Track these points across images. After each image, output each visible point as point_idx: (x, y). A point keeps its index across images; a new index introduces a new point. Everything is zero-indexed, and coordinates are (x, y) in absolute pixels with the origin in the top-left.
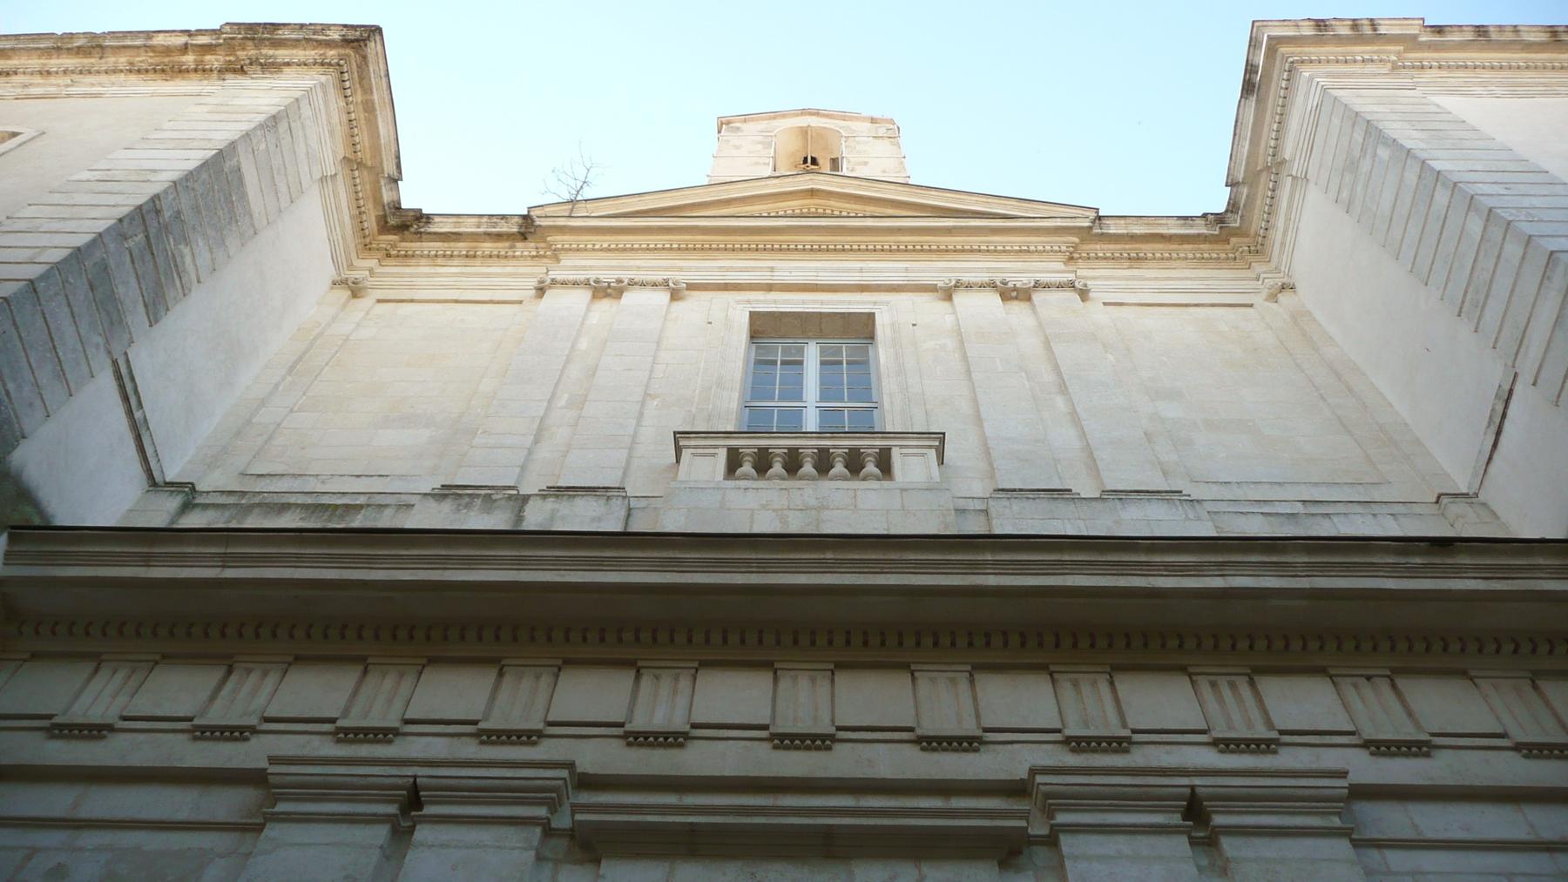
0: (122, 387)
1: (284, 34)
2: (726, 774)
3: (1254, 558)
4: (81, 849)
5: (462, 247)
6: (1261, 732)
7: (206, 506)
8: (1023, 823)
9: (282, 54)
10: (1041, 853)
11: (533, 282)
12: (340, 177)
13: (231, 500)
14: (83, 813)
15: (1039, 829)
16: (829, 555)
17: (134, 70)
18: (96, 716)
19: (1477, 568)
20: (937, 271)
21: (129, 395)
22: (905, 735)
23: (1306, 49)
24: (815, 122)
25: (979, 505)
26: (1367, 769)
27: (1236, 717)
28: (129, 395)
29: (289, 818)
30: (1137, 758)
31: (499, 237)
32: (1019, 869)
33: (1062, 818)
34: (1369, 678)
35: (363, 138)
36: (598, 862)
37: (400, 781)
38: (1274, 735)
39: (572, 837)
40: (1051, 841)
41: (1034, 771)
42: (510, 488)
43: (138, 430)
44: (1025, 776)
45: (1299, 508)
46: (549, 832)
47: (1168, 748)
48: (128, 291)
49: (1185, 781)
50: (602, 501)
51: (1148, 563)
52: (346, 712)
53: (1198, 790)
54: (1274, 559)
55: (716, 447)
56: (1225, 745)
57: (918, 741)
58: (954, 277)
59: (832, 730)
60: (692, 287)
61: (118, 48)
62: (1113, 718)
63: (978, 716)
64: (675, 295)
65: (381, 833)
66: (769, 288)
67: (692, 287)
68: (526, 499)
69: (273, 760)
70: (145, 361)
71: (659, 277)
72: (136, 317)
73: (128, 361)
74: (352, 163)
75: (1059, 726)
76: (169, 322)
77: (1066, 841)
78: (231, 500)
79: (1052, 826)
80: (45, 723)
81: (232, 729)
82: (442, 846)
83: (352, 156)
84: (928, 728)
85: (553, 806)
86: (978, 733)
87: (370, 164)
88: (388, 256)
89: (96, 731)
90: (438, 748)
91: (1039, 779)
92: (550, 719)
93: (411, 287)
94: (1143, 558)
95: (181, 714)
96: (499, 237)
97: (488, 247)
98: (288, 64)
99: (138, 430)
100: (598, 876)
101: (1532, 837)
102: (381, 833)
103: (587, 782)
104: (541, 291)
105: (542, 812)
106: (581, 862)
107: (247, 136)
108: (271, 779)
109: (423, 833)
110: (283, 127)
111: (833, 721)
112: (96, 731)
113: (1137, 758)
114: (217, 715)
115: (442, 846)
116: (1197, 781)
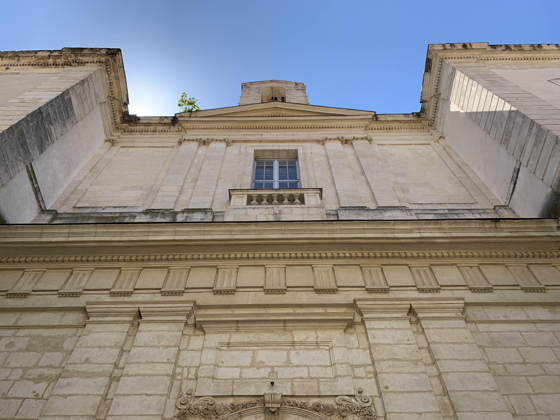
0: (30, 176)
1: (86, 52)
4: (19, 336)
5: (152, 128)
6: (435, 286)
7: (61, 218)
9: (85, 59)
11: (177, 140)
12: (107, 103)
13: (70, 216)
14: (20, 324)
16: (283, 228)
18: (23, 290)
19: (508, 228)
20: (319, 135)
21: (32, 178)
22: (311, 289)
23: (447, 54)
24: (276, 85)
25: (334, 213)
26: (471, 297)
27: (426, 281)
28: (32, 178)
29: (93, 323)
30: (391, 295)
31: (165, 124)
32: (351, 334)
34: (471, 267)
35: (115, 89)
36: (204, 334)
37: (134, 309)
38: (439, 287)
42: (171, 210)
43: (37, 191)
45: (447, 211)
46: (186, 324)
47: (402, 292)
48: (31, 140)
49: (408, 302)
50: (204, 213)
52: (113, 287)
53: (413, 305)
55: (244, 194)
57: (315, 290)
58: (325, 136)
59: (285, 288)
61: (25, 56)
62: (383, 282)
63: (336, 282)
65: (126, 327)
66: (261, 141)
67: (233, 141)
68: (177, 213)
69: (88, 303)
70: (37, 167)
71: (222, 138)
72: (35, 152)
73: (31, 166)
74: (111, 98)
75: (364, 285)
76: (46, 153)
78: (70, 216)
80: (4, 293)
81: (73, 293)
82: (149, 331)
83: (111, 96)
84: (319, 286)
85: (188, 316)
86: (336, 288)
88: (125, 131)
89: (24, 295)
90: (146, 297)
92: (187, 287)
93: (133, 142)
95: (54, 289)
96: (165, 124)
97: (160, 128)
98: (87, 62)
99: (37, 191)
101: (528, 319)
102: (126, 327)
103: (200, 307)
104: (180, 143)
107: (73, 87)
108: (88, 310)
109: (142, 327)
110: (86, 84)
111: (286, 285)
112: (24, 295)
114: (67, 289)
115: (149, 331)
116: (412, 302)
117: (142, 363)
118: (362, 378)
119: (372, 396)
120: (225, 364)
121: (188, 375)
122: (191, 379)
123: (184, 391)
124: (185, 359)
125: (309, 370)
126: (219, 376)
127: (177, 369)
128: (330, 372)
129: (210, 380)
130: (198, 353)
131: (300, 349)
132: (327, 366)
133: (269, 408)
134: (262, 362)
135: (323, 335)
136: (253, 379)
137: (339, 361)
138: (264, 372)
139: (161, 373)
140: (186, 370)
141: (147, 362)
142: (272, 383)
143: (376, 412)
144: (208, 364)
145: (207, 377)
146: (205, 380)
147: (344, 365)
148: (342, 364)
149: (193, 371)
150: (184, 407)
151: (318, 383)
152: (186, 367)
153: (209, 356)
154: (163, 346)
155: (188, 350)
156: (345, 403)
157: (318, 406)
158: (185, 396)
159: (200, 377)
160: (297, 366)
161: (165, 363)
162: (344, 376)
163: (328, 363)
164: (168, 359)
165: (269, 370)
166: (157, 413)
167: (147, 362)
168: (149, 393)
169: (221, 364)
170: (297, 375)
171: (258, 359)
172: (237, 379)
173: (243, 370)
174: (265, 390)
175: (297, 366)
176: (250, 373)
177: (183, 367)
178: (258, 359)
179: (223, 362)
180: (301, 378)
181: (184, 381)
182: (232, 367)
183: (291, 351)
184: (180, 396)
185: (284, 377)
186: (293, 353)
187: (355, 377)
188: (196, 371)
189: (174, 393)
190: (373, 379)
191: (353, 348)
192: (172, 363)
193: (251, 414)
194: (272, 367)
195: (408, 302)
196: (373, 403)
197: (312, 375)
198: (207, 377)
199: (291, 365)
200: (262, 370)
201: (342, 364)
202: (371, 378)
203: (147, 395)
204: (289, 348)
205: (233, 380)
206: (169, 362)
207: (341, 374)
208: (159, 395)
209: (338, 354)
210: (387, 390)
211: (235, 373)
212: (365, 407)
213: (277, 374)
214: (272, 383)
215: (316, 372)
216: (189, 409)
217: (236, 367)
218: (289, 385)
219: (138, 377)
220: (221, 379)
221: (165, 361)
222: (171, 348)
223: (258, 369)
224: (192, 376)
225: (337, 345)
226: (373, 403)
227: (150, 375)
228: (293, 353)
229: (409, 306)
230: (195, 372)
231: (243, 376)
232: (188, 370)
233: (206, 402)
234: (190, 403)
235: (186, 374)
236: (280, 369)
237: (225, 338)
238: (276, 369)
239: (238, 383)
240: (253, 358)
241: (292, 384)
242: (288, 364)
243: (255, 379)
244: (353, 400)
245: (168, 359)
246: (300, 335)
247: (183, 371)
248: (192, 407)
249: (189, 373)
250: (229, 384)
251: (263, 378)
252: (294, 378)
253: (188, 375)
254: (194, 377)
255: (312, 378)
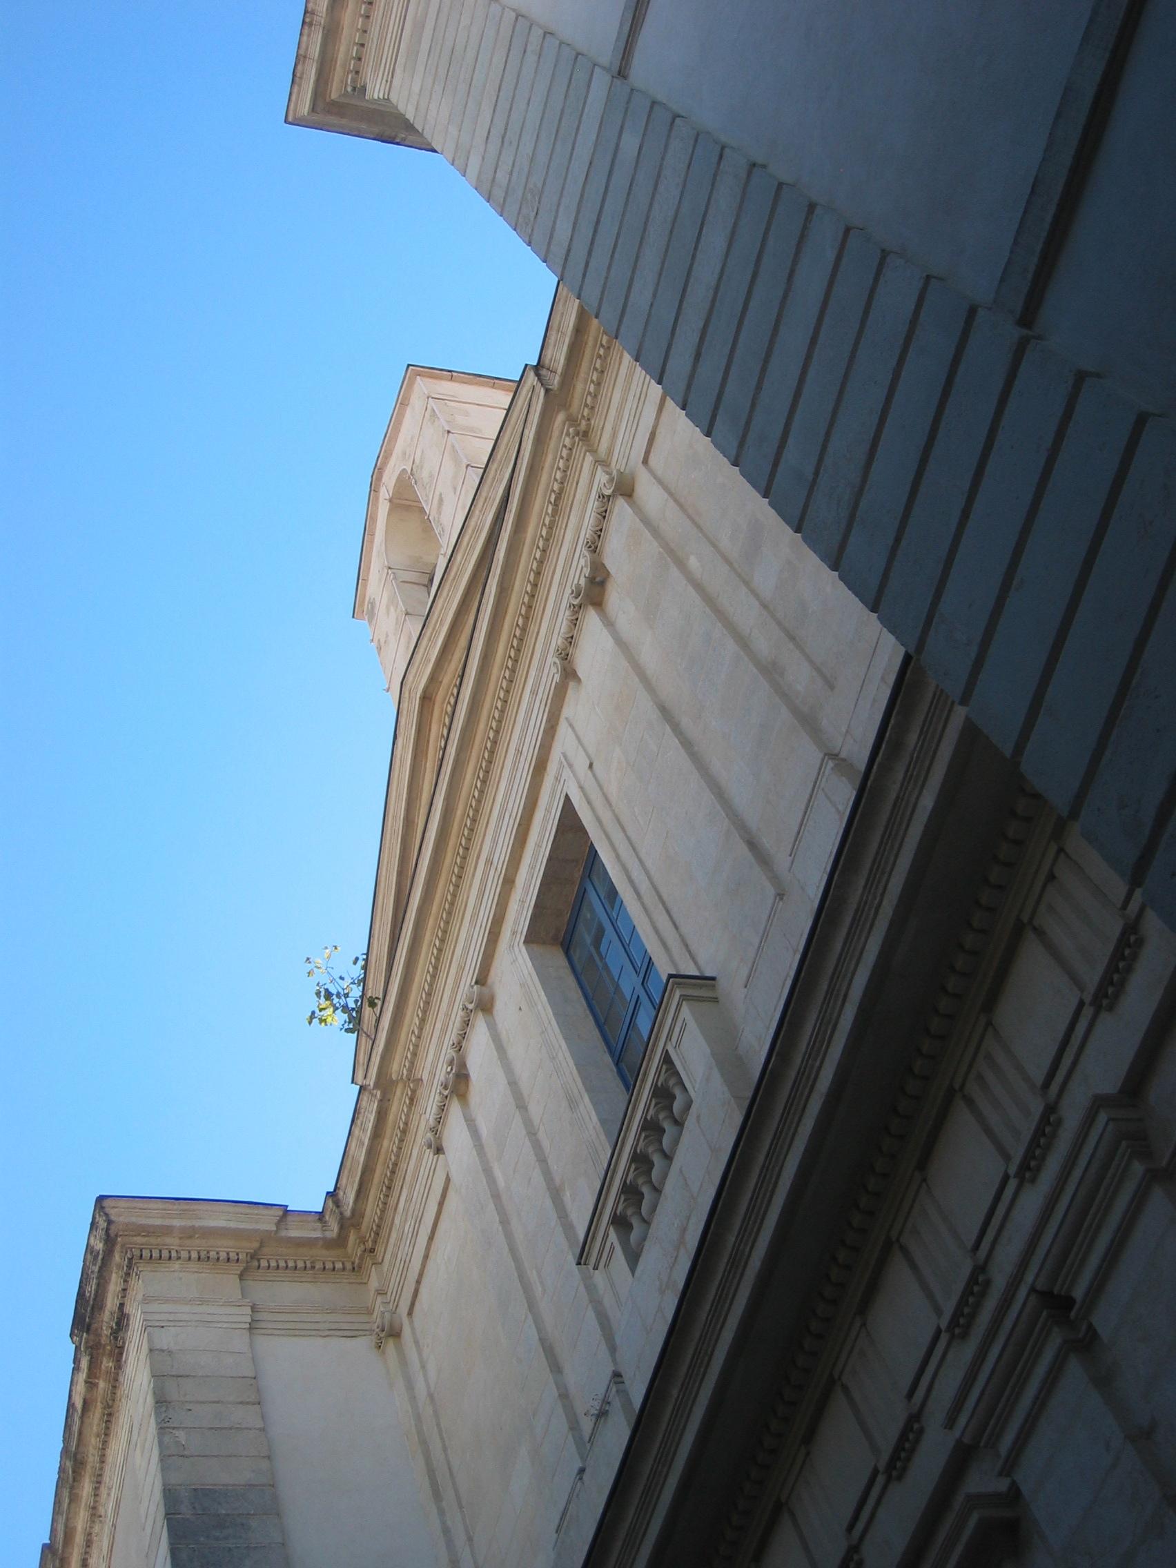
1: (91, 1289)
3: (838, 946)
9: (111, 1303)
11: (429, 1153)
17: (106, 1434)
20: (540, 671)
23: (341, 56)
24: (384, 494)
30: (999, 1282)
35: (224, 1247)
49: (1023, 1292)
51: (800, 1074)
53: (1038, 1287)
54: (848, 920)
55: (606, 1235)
56: (1028, 1169)
58: (552, 658)
60: (481, 980)
61: (79, 1440)
64: (485, 1005)
66: (509, 882)
67: (481, 980)
71: (458, 1016)
83: (242, 1266)
87: (257, 1248)
88: (372, 1251)
93: (406, 1264)
94: (792, 1074)
98: (122, 1305)
113: (999, 1282)
116: (1029, 1278)
195: (1023, 1292)
229: (1033, 1298)
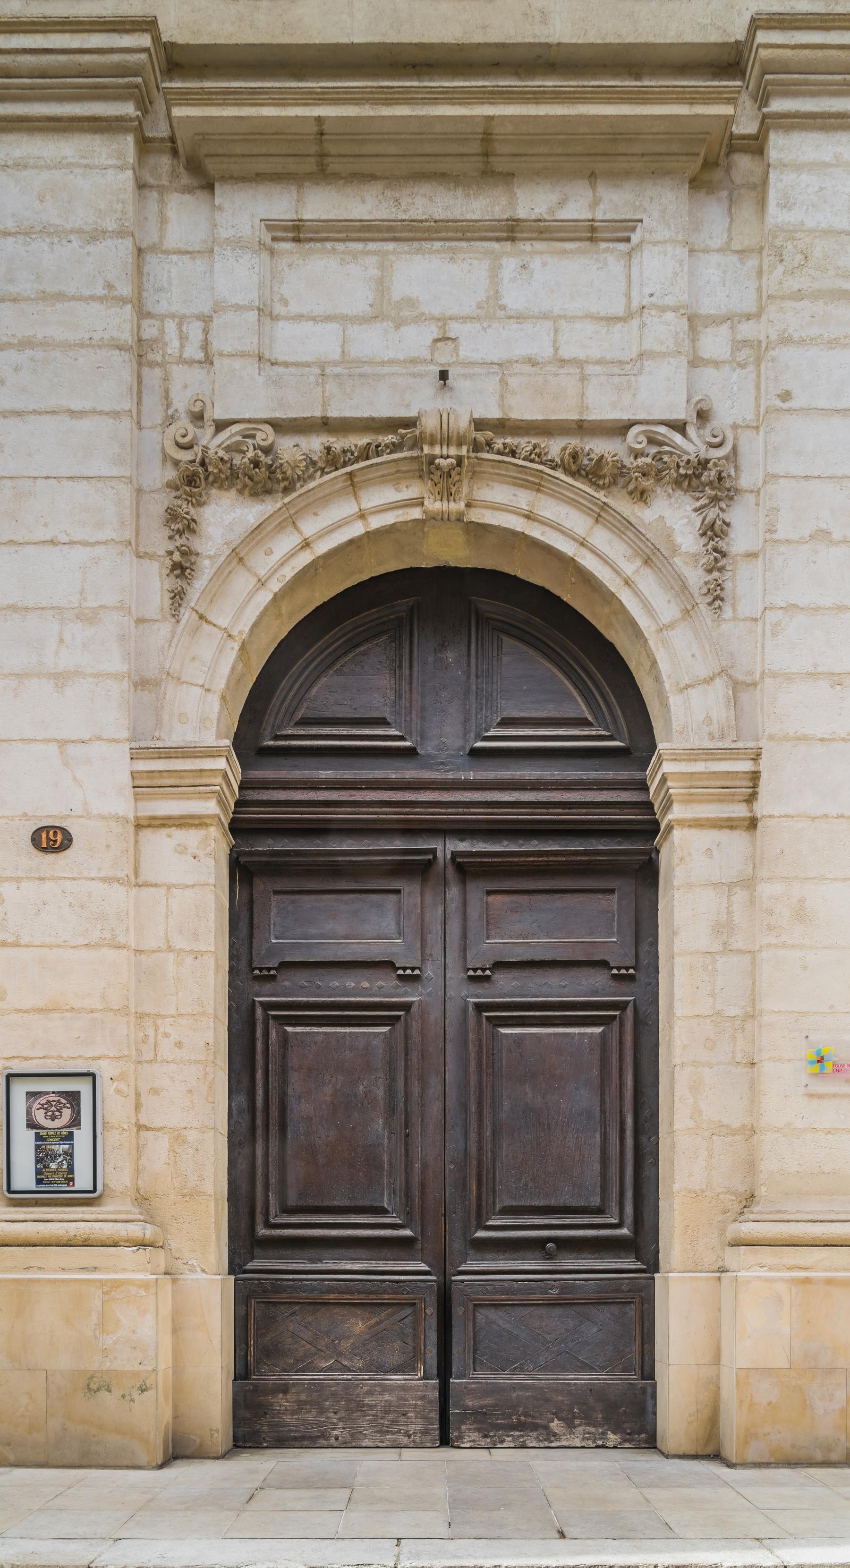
2: (358, 39)
8: (726, 110)
10: (743, 163)
15: (746, 126)
33: (778, 105)
36: (209, 187)
39: (175, 152)
40: (756, 146)
41: (756, 24)
44: (739, 33)
46: (145, 145)
77: (779, 145)
79: (765, 117)
91: (762, 37)
100: (214, 208)
105: (128, 109)
106: (188, 190)
117: (28, 299)
118: (716, 364)
119: (735, 427)
120: (294, 308)
121: (182, 346)
122: (191, 362)
123: (181, 403)
124: (161, 289)
125: (556, 331)
126: (280, 353)
127: (146, 323)
128: (620, 342)
129: (251, 367)
130: (200, 265)
131: (533, 253)
132: (617, 319)
133: (434, 457)
134: (411, 302)
135: (612, 202)
136: (383, 363)
137: (654, 300)
138: (416, 340)
139: (97, 337)
140: (171, 326)
141: (44, 297)
142: (443, 375)
143: (737, 478)
144: (238, 308)
145: (243, 355)
146: (237, 364)
147: (670, 316)
148: (664, 309)
149: (195, 331)
150: (185, 456)
151: (583, 379)
152: (173, 316)
153: (237, 277)
154: (80, 232)
155: (167, 252)
156: (653, 450)
157: (575, 456)
158: (184, 423)
159: (221, 354)
160: (520, 318)
161: (101, 299)
162: (663, 355)
163: (619, 309)
164: (110, 286)
165: (432, 331)
166: (115, 472)
167: (44, 297)
168: (73, 407)
169: (279, 309)
170: (522, 349)
171: (399, 289)
172: (336, 364)
173: (354, 331)
174: (421, 402)
175: (520, 318)
176: (371, 342)
177: (162, 318)
178: (399, 289)
179: (285, 302)
180: (532, 362)
181: (174, 367)
182: (314, 319)
183: (504, 261)
184: (170, 420)
185: (477, 357)
186: (510, 265)
187: (696, 362)
188: (206, 332)
189: (154, 413)
190: (751, 368)
191: (706, 251)
192: (123, 301)
193: (383, 480)
194: (443, 320)
196: (734, 449)
197: (566, 352)
198: (243, 355)
199: (500, 313)
200: (410, 332)
201: (664, 309)
202: (742, 366)
203: (72, 413)
204: (496, 246)
205: (322, 366)
206: (111, 298)
207: (657, 348)
208: (107, 414)
209: (658, 266)
210: (785, 406)
211: (323, 342)
212: (707, 461)
213: (456, 349)
214: (443, 375)
215: (579, 342)
216: (203, 464)
217: (329, 318)
218: (492, 384)
219: (29, 352)
220: (286, 364)
221: (100, 291)
222: (109, 242)
223: (398, 327)
224: (193, 351)
225: (659, 237)
226: (734, 449)
227: (67, 346)
228: (510, 265)
230: (201, 337)
231: (355, 351)
232: (180, 326)
233: (250, 441)
234: (204, 442)
235: (176, 343)
236: (468, 327)
237: (280, 204)
238: (454, 329)
239: (337, 376)
240: (382, 286)
241: (503, 382)
242: (492, 310)
243: (391, 362)
244: (678, 438)
245: (110, 286)
246: (533, 202)
247: (162, 331)
248: (211, 452)
249: (183, 338)
250: (312, 379)
251: (413, 361)
252: (510, 362)
253: (182, 346)
254: (200, 355)
255: (563, 362)
